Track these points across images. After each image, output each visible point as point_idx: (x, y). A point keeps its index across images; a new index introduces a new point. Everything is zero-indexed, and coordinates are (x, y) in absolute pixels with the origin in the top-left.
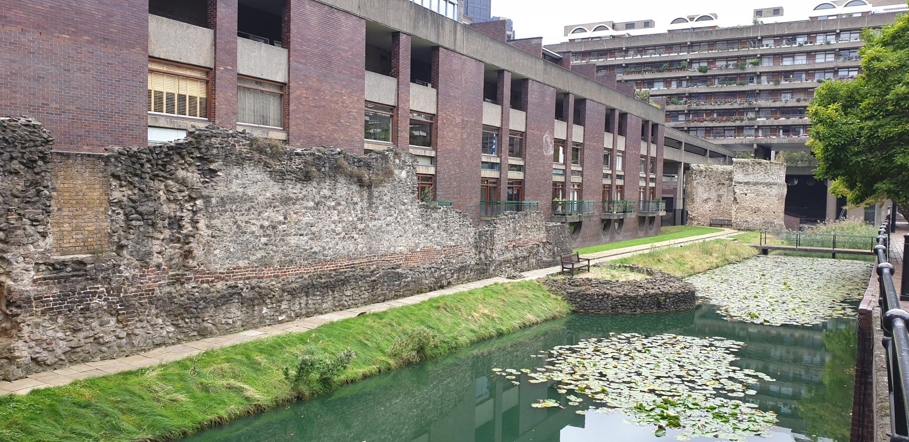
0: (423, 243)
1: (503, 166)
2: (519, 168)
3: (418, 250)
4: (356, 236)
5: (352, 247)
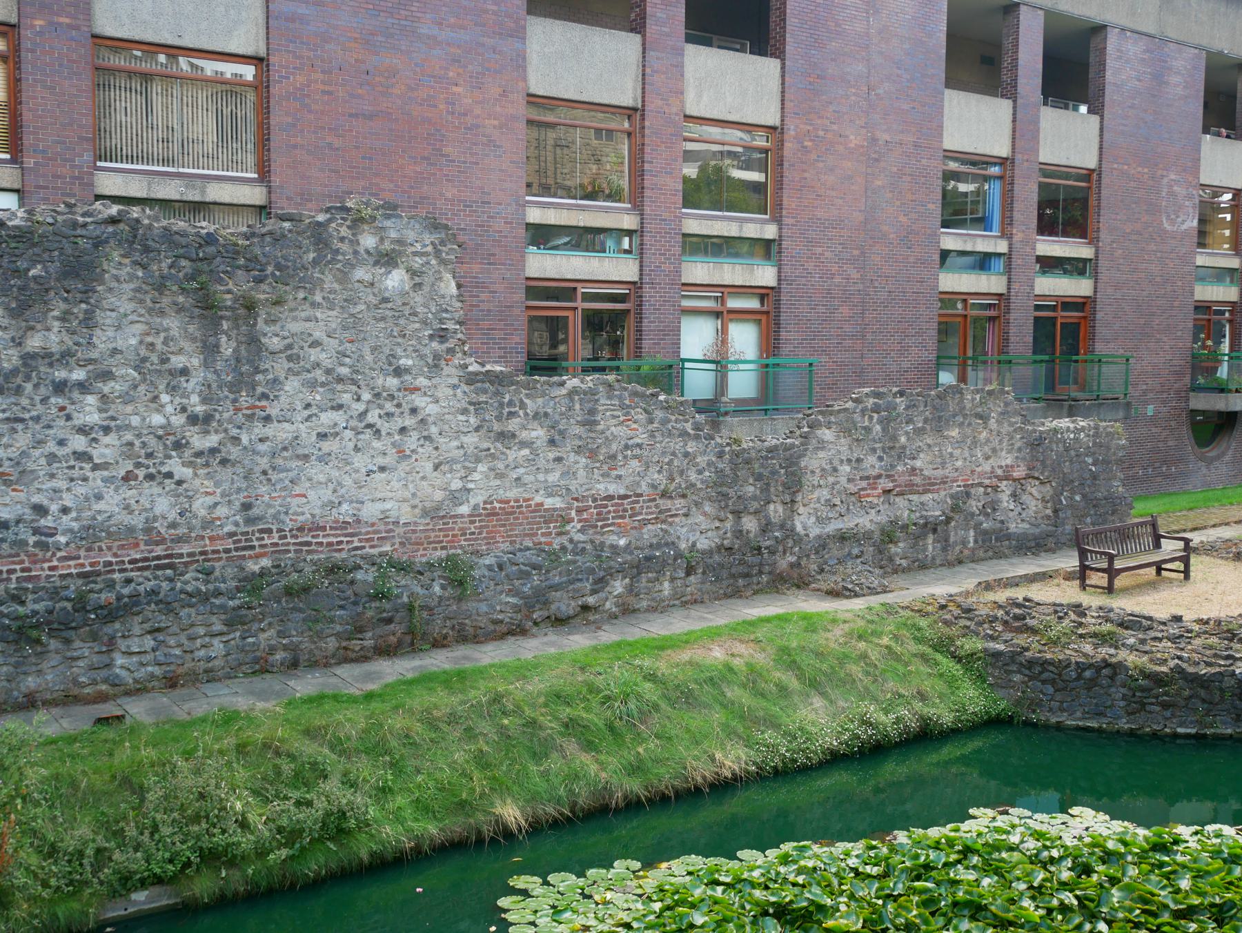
0: (482, 488)
1: (1016, 261)
2: (1075, 267)
3: (464, 509)
4: (181, 471)
5: (164, 506)
